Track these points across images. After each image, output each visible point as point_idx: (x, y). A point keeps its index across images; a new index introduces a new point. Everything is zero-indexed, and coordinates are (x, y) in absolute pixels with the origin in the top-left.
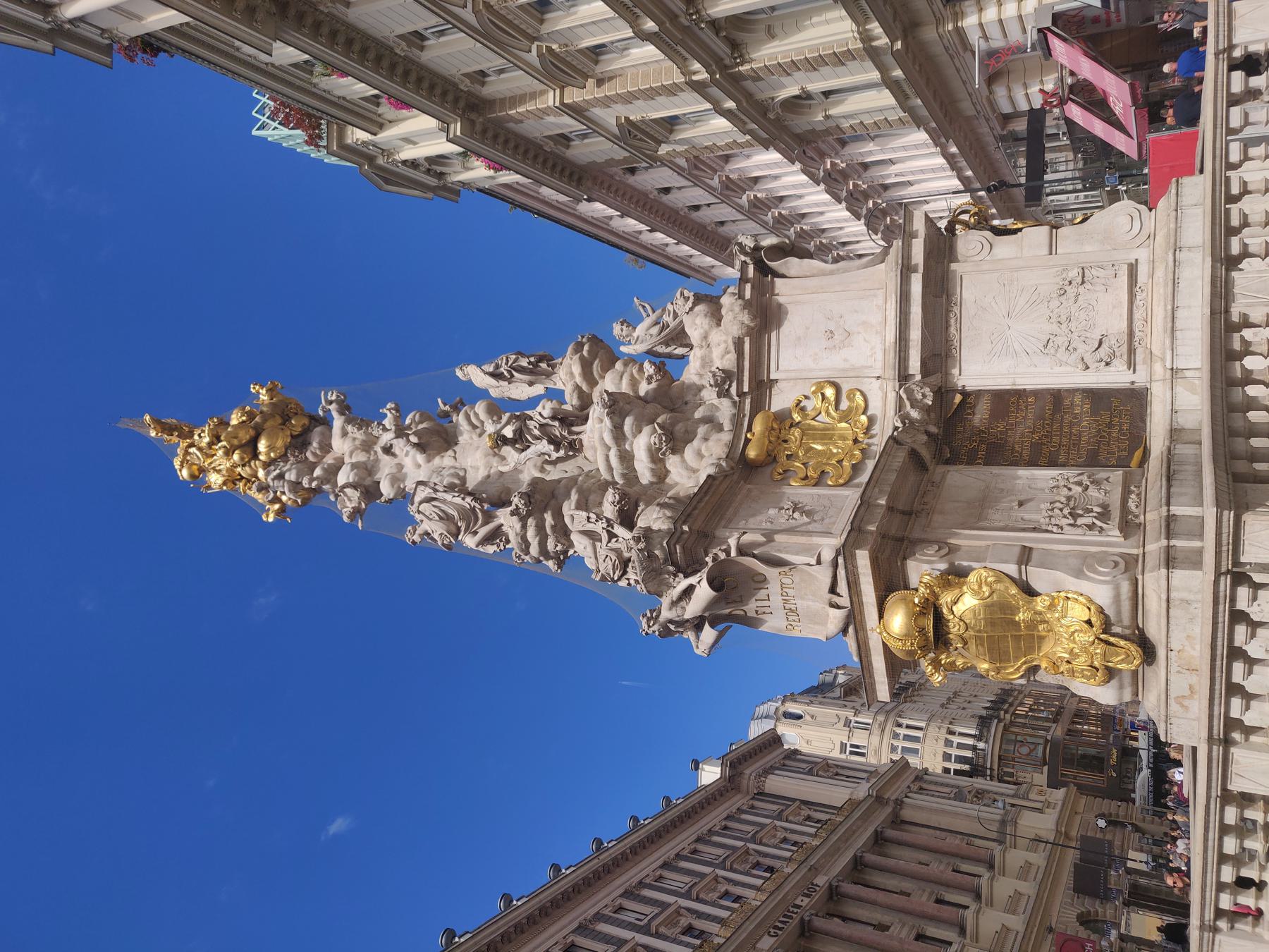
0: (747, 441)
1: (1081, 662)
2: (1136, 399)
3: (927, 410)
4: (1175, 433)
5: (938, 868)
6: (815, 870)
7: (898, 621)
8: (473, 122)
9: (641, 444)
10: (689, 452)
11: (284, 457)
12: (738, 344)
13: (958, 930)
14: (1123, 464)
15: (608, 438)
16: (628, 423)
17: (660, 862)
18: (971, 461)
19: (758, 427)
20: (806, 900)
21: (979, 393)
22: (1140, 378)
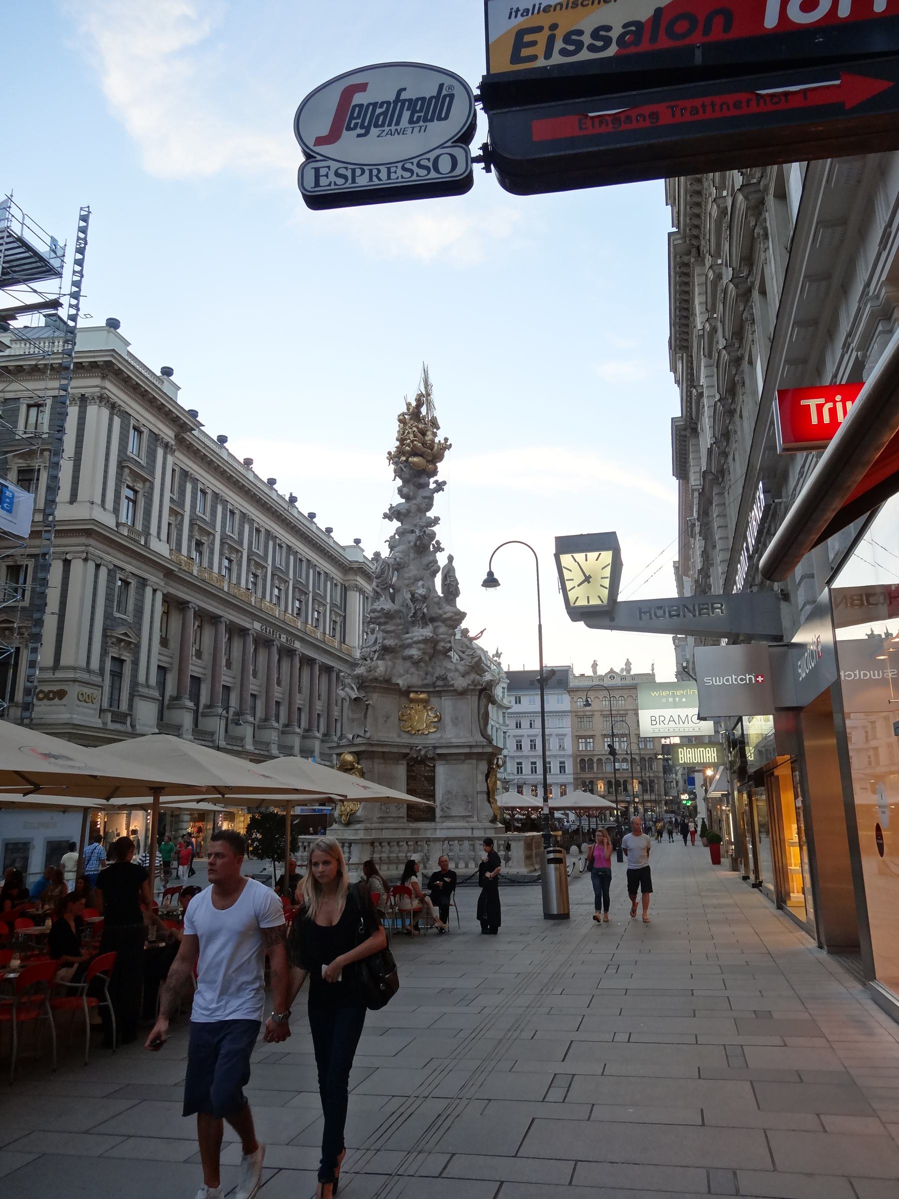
0: (416, 692)
1: (343, 808)
2: (432, 819)
3: (426, 755)
4: (414, 830)
5: (319, 706)
6: (302, 640)
7: (349, 758)
8: (685, 430)
9: (414, 652)
10: (413, 670)
11: (411, 468)
12: (453, 685)
13: (286, 722)
14: (408, 816)
15: (415, 639)
16: (422, 646)
17: (290, 544)
18: (409, 770)
19: (422, 696)
20: (284, 640)
21: (434, 771)
22: (437, 819)
